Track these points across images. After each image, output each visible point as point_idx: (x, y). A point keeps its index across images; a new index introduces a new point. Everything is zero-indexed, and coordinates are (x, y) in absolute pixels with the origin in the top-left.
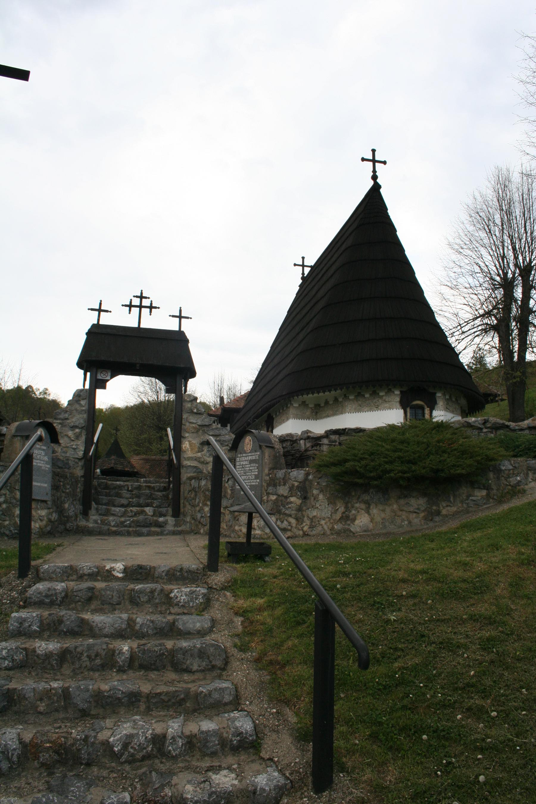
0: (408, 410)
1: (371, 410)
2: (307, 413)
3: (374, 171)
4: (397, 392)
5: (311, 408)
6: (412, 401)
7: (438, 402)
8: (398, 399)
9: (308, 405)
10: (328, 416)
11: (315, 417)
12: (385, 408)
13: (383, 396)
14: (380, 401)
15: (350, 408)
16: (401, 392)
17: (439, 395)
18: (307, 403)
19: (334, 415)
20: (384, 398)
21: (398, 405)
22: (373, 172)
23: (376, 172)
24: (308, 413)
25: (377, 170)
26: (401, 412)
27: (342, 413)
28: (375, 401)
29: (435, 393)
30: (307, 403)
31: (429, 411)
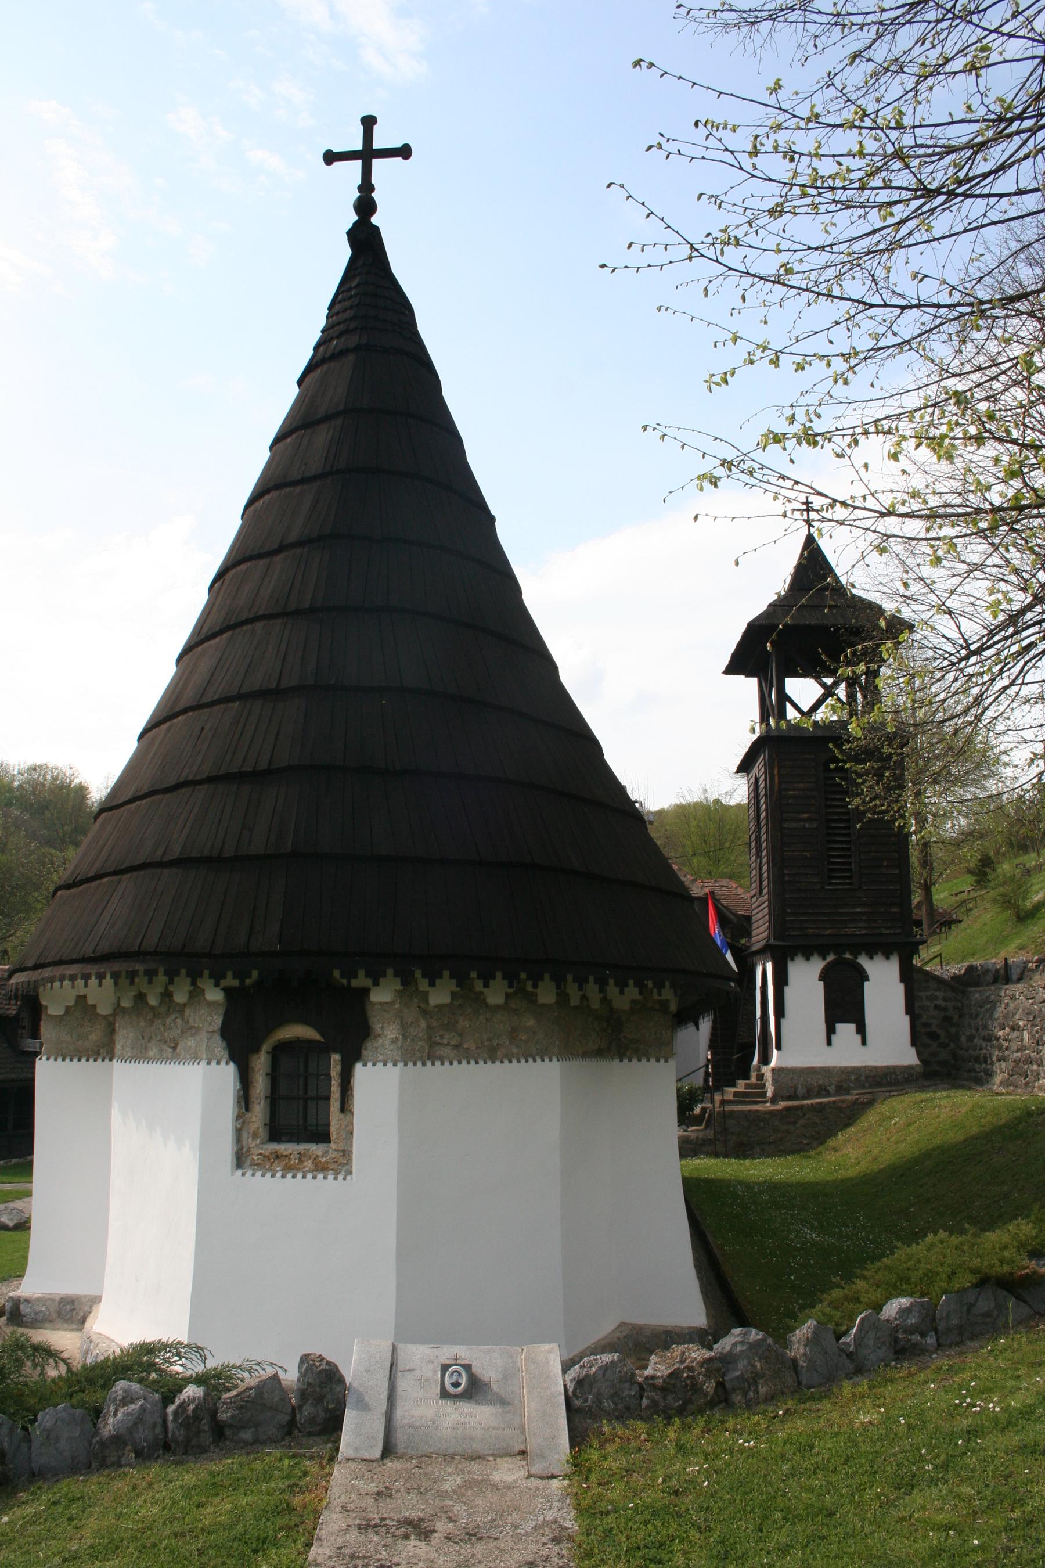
0: (261, 1063)
1: (161, 1058)
2: (93, 1037)
3: (366, 187)
4: (214, 995)
5: (105, 1017)
6: (269, 1031)
7: (377, 1027)
8: (218, 1021)
9: (94, 1006)
13: (185, 1005)
16: (228, 991)
17: (382, 995)
18: (90, 1002)
20: (187, 1011)
21: (219, 1046)
22: (360, 188)
23: (372, 188)
25: (374, 181)
26: (228, 1072)
28: (168, 1021)
29: (365, 992)
30: (90, 1002)
31: (339, 1067)
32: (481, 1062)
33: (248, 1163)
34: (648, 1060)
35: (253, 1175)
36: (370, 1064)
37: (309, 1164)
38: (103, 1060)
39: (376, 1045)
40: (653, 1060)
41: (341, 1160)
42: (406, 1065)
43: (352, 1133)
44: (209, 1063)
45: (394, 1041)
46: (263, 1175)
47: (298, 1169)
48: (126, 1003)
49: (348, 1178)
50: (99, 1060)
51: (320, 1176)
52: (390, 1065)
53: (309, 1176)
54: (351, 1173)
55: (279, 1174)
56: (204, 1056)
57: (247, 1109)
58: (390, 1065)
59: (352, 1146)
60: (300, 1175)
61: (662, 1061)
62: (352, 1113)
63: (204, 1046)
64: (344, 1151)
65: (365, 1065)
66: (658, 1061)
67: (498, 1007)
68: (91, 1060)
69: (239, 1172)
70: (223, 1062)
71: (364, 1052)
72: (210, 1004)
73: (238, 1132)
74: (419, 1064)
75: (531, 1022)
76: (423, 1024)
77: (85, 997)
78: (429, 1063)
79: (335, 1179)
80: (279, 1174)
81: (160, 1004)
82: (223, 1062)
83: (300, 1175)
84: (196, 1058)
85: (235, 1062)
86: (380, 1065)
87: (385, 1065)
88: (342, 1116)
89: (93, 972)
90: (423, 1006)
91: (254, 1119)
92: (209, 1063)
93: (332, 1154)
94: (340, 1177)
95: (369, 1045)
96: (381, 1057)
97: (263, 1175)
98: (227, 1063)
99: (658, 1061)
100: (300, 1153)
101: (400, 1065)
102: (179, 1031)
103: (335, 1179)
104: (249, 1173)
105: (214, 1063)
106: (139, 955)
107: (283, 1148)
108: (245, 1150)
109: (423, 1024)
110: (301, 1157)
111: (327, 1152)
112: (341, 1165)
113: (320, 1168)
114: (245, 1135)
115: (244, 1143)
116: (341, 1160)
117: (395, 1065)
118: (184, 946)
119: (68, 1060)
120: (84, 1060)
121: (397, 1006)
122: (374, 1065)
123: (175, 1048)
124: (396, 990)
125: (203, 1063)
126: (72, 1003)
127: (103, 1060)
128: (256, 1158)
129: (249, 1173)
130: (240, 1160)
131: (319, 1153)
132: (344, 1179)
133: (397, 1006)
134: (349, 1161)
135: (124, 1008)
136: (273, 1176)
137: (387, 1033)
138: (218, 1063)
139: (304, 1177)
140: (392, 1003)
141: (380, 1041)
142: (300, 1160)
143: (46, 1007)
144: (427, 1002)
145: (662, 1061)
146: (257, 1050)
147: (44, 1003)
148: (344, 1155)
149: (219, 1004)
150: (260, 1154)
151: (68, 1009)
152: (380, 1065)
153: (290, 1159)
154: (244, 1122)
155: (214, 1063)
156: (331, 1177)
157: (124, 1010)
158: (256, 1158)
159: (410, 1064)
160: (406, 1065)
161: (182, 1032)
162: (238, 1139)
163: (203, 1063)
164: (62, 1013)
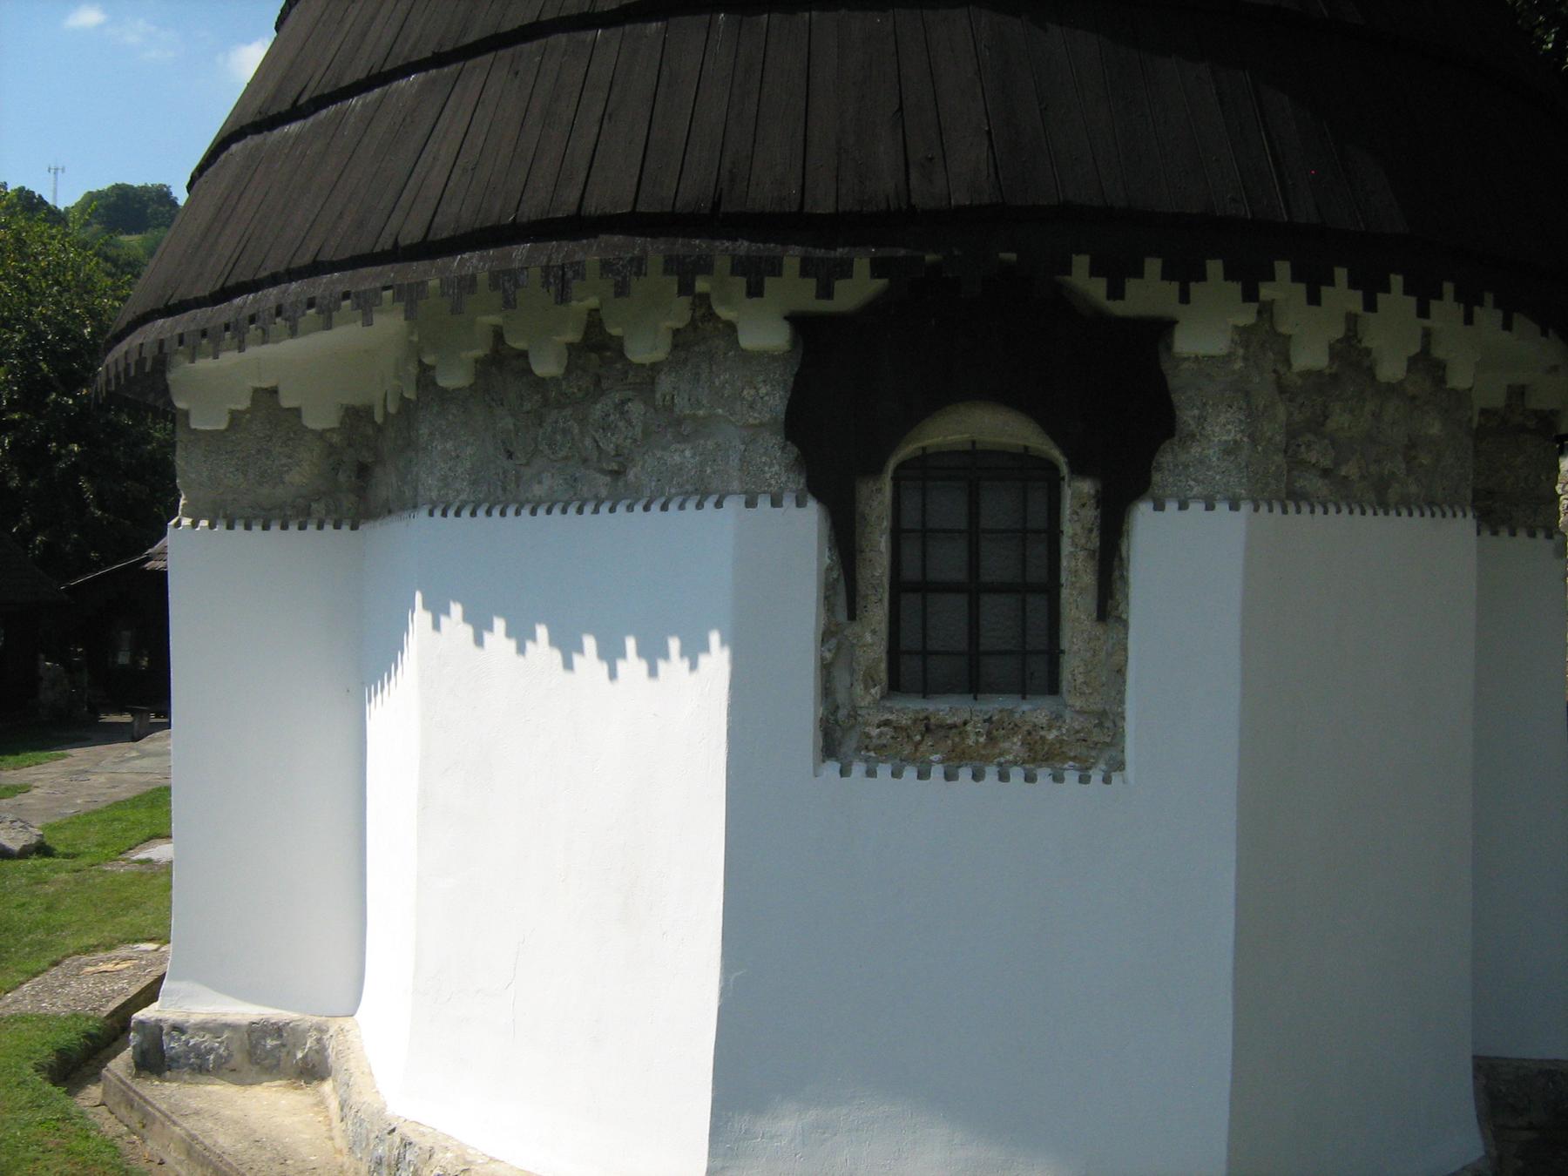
0: (877, 502)
1: (574, 498)
4: (764, 333)
5: (321, 435)
7: (1187, 416)
8: (773, 400)
9: (296, 412)
12: (659, 496)
13: (655, 367)
14: (636, 409)
16: (800, 323)
18: (286, 402)
20: (665, 383)
21: (774, 460)
24: (301, 474)
26: (801, 528)
28: (598, 410)
29: (1163, 328)
31: (1091, 514)
32: (1369, 512)
33: (851, 742)
34: (1513, 534)
35: (871, 773)
36: (1172, 506)
37: (1014, 746)
38: (320, 527)
39: (1183, 457)
40: (1522, 535)
41: (1097, 736)
42: (1256, 509)
43: (1121, 672)
44: (751, 503)
45: (1230, 450)
46: (896, 774)
47: (987, 759)
48: (454, 378)
49: (1116, 777)
50: (312, 528)
51: (1043, 774)
52: (1222, 508)
53: (1017, 774)
54: (1120, 766)
55: (937, 771)
56: (736, 485)
57: (852, 616)
58: (1222, 508)
59: (1122, 702)
60: (991, 772)
61: (1541, 535)
62: (1125, 624)
63: (734, 461)
64: (1104, 713)
65: (1159, 507)
66: (1532, 535)
67: (1393, 389)
68: (293, 528)
69: (832, 767)
70: (789, 501)
71: (1156, 477)
72: (747, 357)
73: (826, 670)
74: (1277, 509)
75: (1435, 429)
76: (1281, 412)
77: (274, 392)
78: (1291, 508)
79: (1084, 779)
80: (937, 771)
81: (568, 370)
82: (789, 501)
83: (991, 772)
84: (702, 491)
85: (820, 498)
86: (1196, 508)
87: (1210, 507)
88: (1099, 630)
89: (434, 283)
90: (1282, 369)
91: (868, 638)
92: (751, 503)
93: (1072, 722)
94: (1096, 775)
95: (1165, 458)
96: (1197, 490)
97: (896, 774)
98: (800, 503)
99: (1532, 535)
100: (989, 720)
101: (1246, 508)
102: (639, 430)
103: (1084, 779)
104: (858, 769)
105: (764, 503)
106: (579, 226)
107: (943, 708)
108: (842, 713)
109: (1281, 412)
110: (995, 730)
111: (1059, 717)
112: (1096, 746)
113: (1042, 756)
114: (842, 678)
115: (841, 697)
116: (1097, 736)
117: (1234, 507)
118: (716, 204)
119: (239, 528)
120: (275, 528)
121: (1238, 365)
122: (1183, 506)
123: (617, 474)
124: (1236, 327)
125: (734, 504)
126: (244, 404)
127: (320, 527)
128: (875, 732)
129: (858, 769)
130: (835, 740)
131: (1042, 718)
132: (1107, 780)
133: (1238, 365)
134: (1116, 739)
135: (444, 390)
136: (923, 775)
137: (1213, 431)
138: (776, 502)
139: (1004, 777)
140: (1228, 358)
141: (1195, 450)
142: (991, 739)
143: (186, 414)
144: (1287, 362)
145: (1541, 535)
146: (876, 471)
147: (180, 404)
148: (1100, 725)
150: (887, 723)
151: (235, 416)
152: (1196, 508)
153: (963, 735)
154: (839, 647)
155: (764, 503)
156: (1071, 777)
157: (445, 396)
158: (875, 732)
159: (1264, 508)
160: (1256, 509)
161: (646, 434)
162: (827, 691)
163: (734, 504)
164: (223, 426)
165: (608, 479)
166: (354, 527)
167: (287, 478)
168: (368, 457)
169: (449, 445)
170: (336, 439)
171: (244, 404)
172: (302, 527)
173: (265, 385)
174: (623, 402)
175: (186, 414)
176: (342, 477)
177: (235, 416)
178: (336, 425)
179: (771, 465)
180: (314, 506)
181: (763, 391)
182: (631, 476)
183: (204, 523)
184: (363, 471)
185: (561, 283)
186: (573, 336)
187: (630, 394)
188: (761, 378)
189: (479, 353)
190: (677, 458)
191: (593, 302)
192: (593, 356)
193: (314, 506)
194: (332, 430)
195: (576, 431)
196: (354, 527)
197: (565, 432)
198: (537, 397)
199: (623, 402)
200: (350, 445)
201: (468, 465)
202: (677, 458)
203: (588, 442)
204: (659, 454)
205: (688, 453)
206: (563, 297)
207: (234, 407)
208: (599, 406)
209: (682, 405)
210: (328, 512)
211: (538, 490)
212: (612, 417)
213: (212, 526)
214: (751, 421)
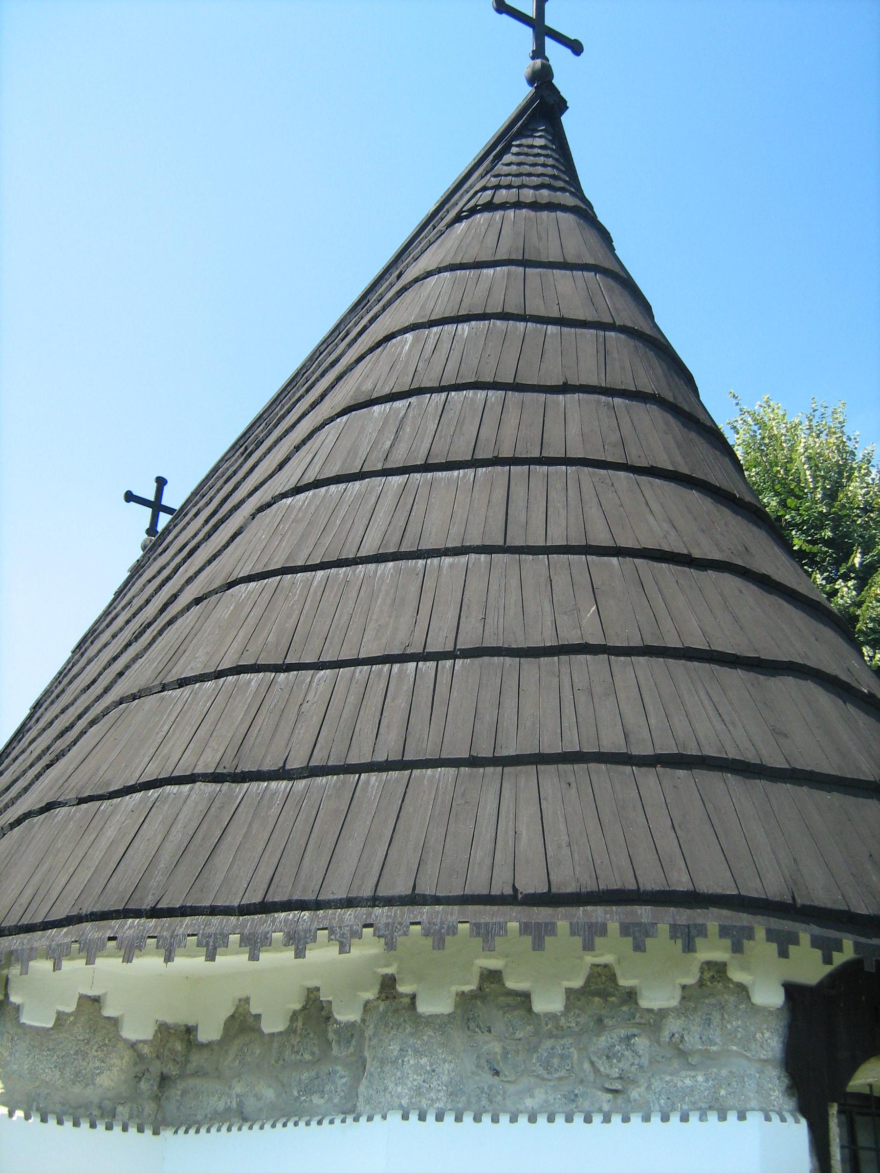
5: (133, 1045)
8: (770, 1042)
9: (115, 1022)
10: (240, 1116)
11: (149, 1107)
13: (662, 1014)
14: (642, 1043)
15: (413, 1080)
18: (109, 1011)
19: (288, 1112)
20: (673, 1025)
24: (111, 1077)
27: (350, 1110)
30: (109, 1011)
48: (435, 1004)
50: (117, 1129)
56: (753, 1103)
81: (568, 1007)
102: (645, 1061)
126: (70, 1008)
149: (770, 1012)
151: (61, 1017)
163: (755, 1118)
164: (50, 1025)
165: (610, 1096)
166: (156, 1132)
167: (98, 1080)
168: (172, 1070)
169: (424, 1061)
170: (146, 1050)
171: (70, 1008)
172: (109, 1127)
173: (91, 993)
174: (628, 1038)
175: (18, 1008)
176: (144, 1085)
177: (61, 1017)
178: (151, 1038)
179: (774, 1092)
180: (120, 1109)
181: (767, 1035)
182: (634, 1094)
183: (19, 1114)
184: (164, 1080)
185: (688, 938)
186: (577, 983)
187: (636, 1031)
188: (765, 1026)
189: (467, 988)
190: (688, 1082)
191: (608, 958)
192: (597, 999)
193: (120, 1109)
194: (145, 1042)
195: (575, 1057)
196: (156, 1132)
197: (563, 1057)
198: (530, 1028)
199: (628, 1038)
200: (158, 1057)
201: (445, 1079)
202: (688, 1082)
203: (587, 1066)
204: (668, 1078)
205: (700, 1078)
206: (689, 948)
207: (62, 1008)
208: (603, 1038)
209: (692, 1041)
210: (131, 1117)
211: (529, 1103)
212: (618, 1048)
213: (27, 1117)
214: (762, 1057)
